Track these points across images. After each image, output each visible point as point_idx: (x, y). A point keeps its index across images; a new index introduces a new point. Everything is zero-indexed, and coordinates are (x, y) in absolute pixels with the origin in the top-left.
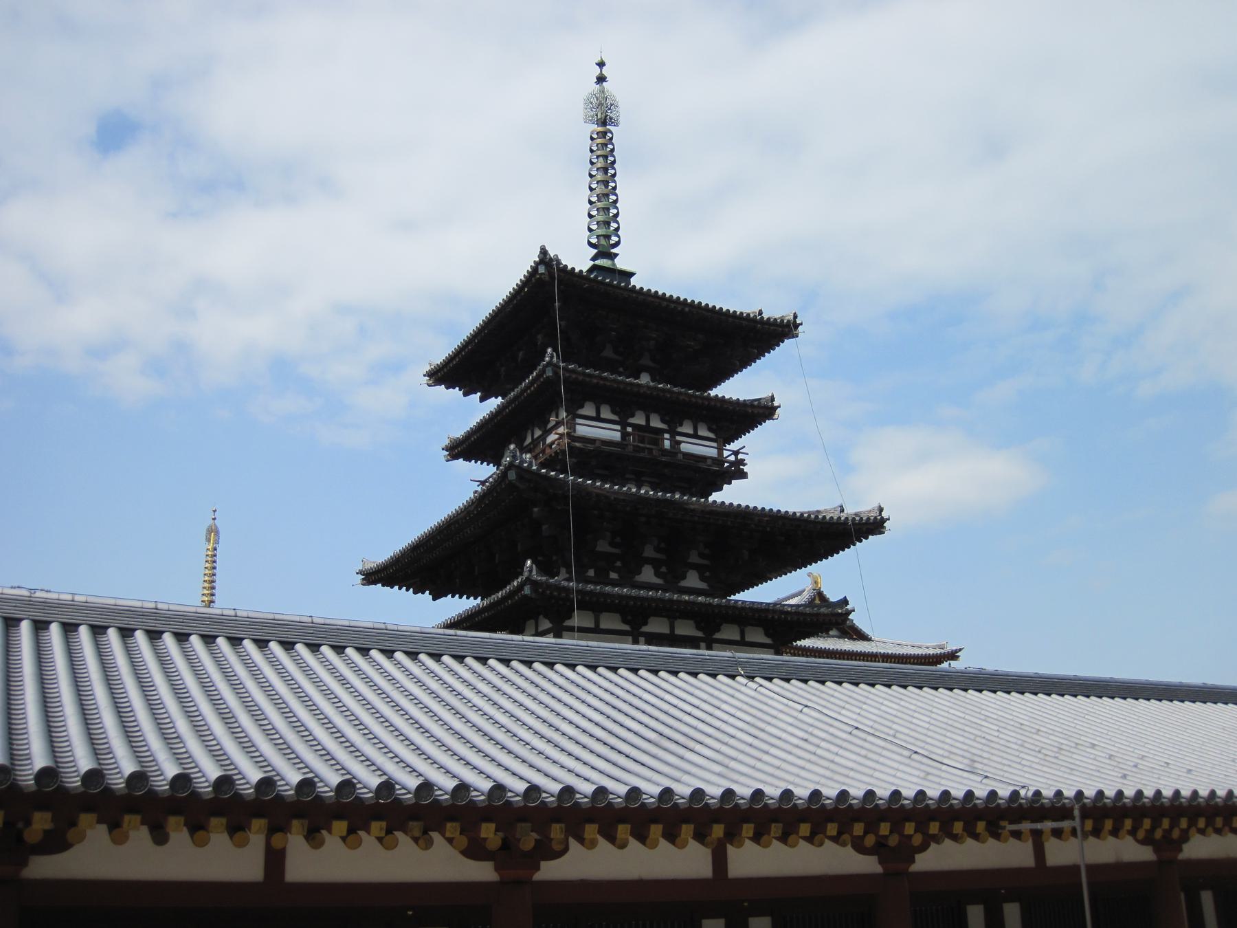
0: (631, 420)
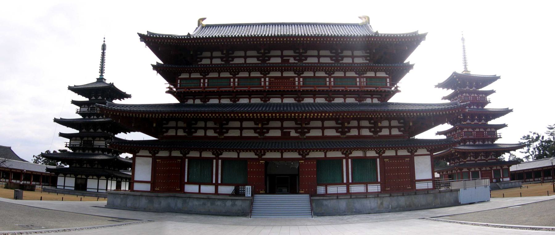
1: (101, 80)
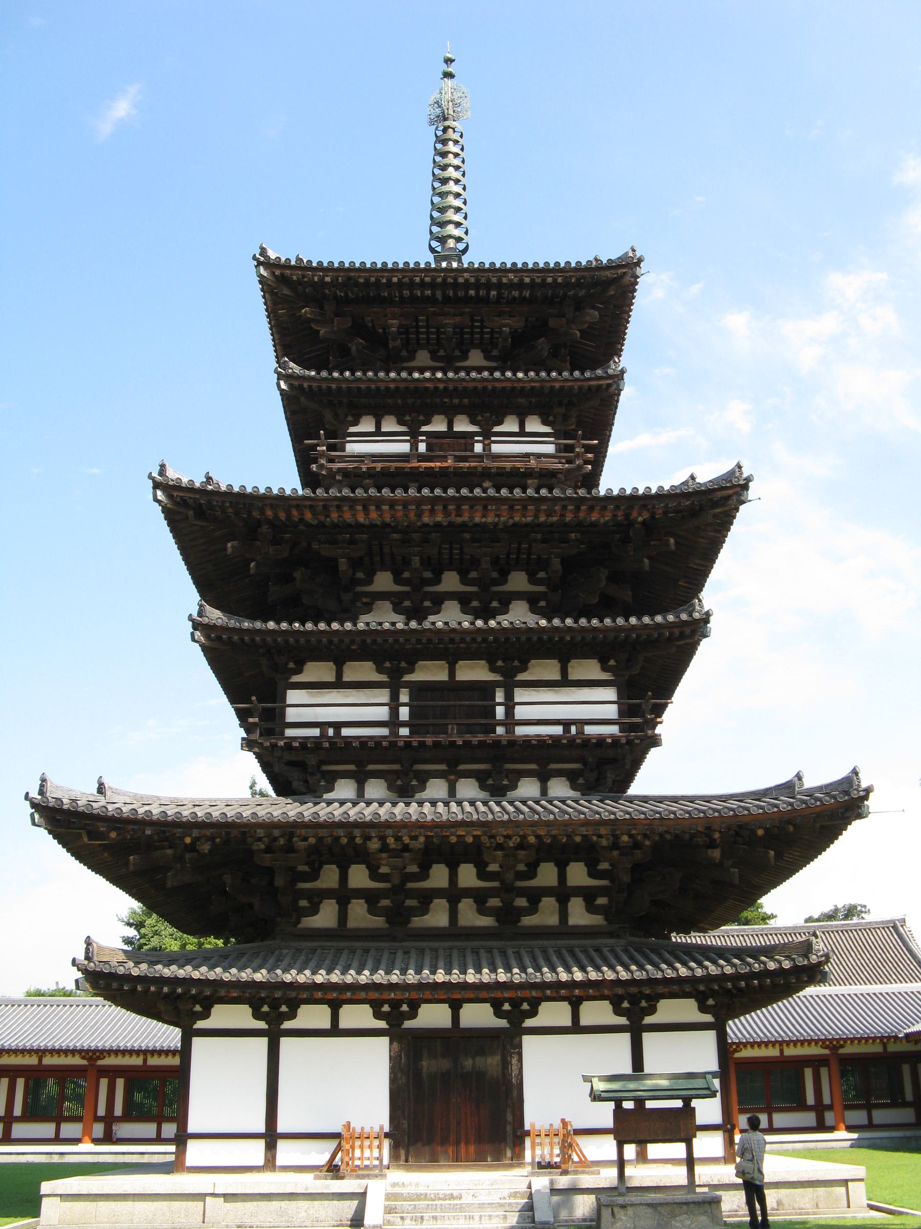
0: (424, 429)
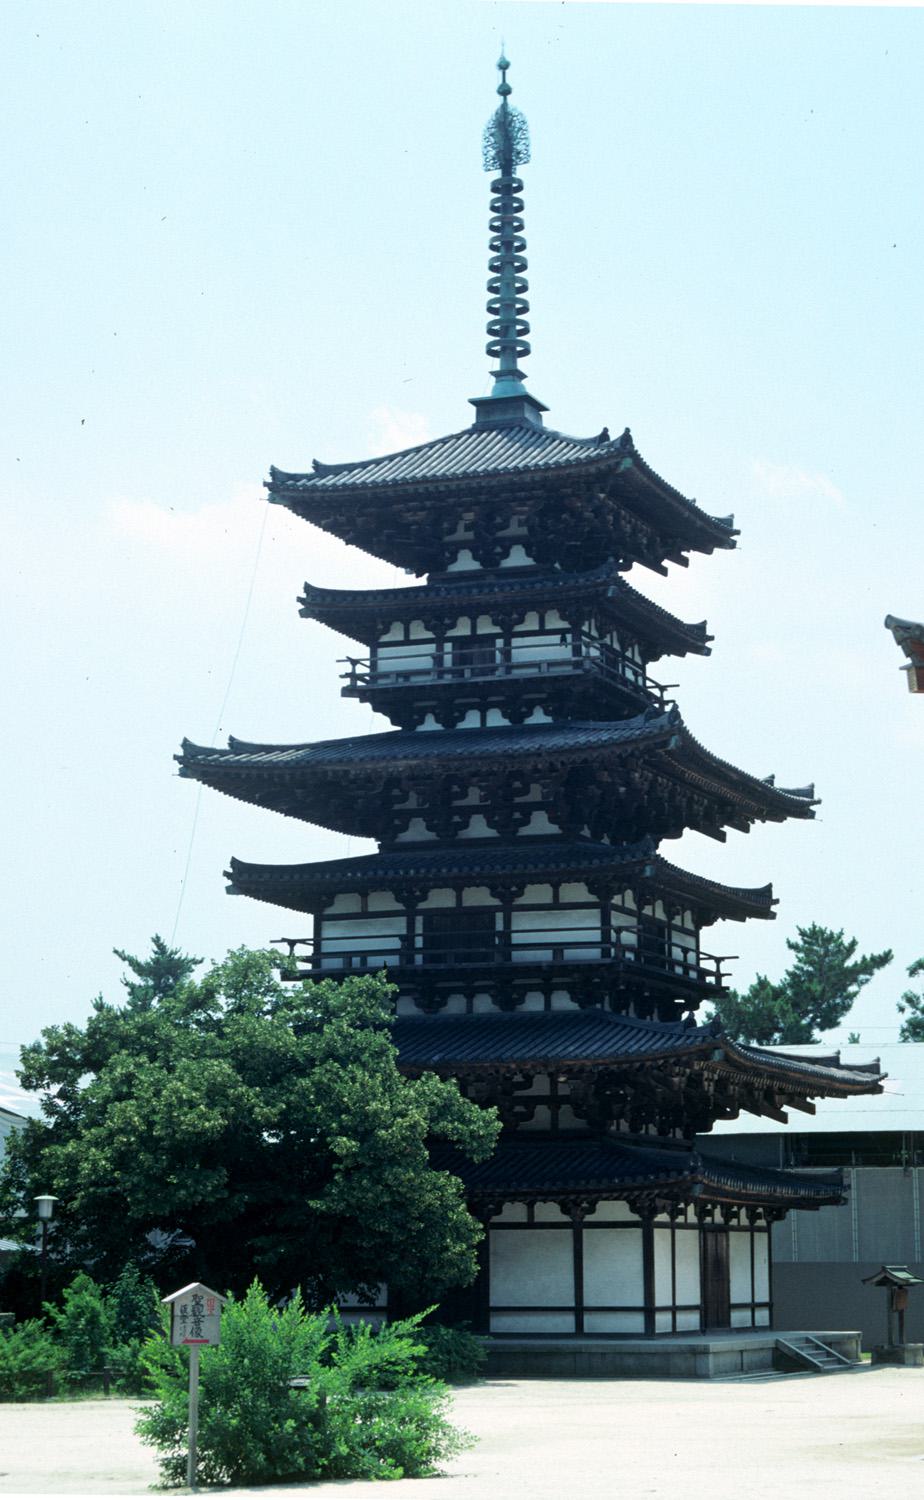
0: (451, 633)
1: (507, 412)
